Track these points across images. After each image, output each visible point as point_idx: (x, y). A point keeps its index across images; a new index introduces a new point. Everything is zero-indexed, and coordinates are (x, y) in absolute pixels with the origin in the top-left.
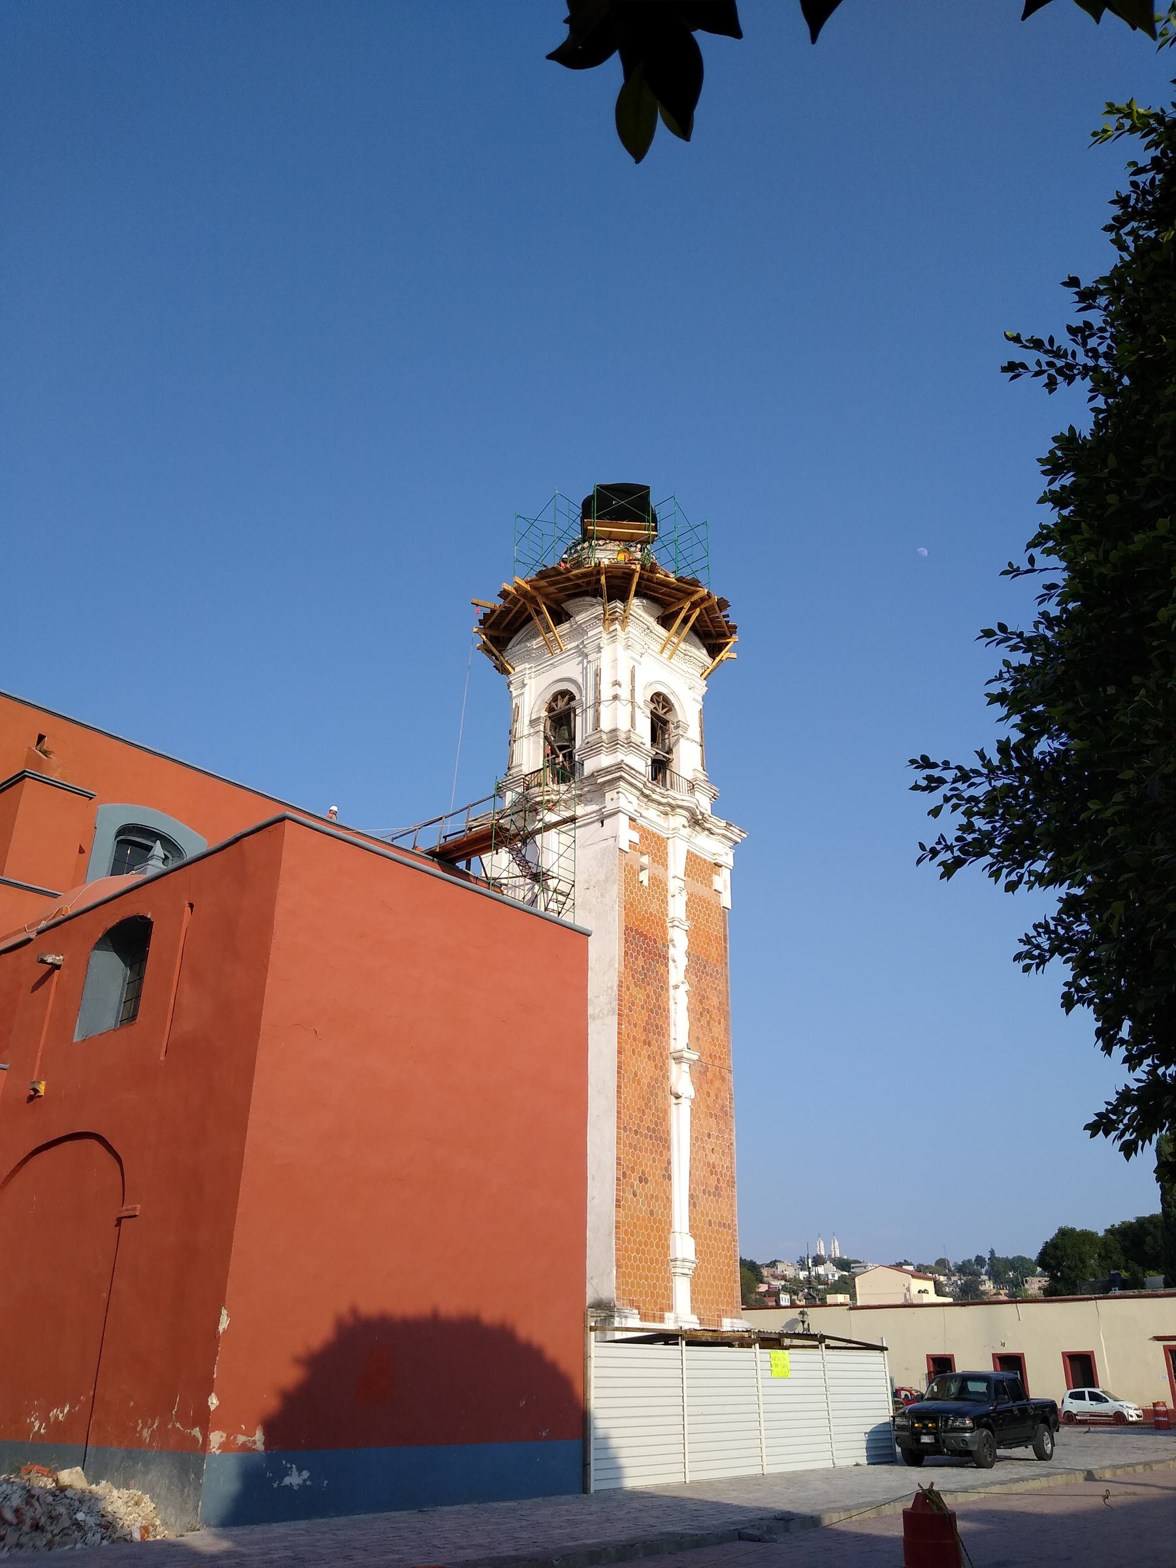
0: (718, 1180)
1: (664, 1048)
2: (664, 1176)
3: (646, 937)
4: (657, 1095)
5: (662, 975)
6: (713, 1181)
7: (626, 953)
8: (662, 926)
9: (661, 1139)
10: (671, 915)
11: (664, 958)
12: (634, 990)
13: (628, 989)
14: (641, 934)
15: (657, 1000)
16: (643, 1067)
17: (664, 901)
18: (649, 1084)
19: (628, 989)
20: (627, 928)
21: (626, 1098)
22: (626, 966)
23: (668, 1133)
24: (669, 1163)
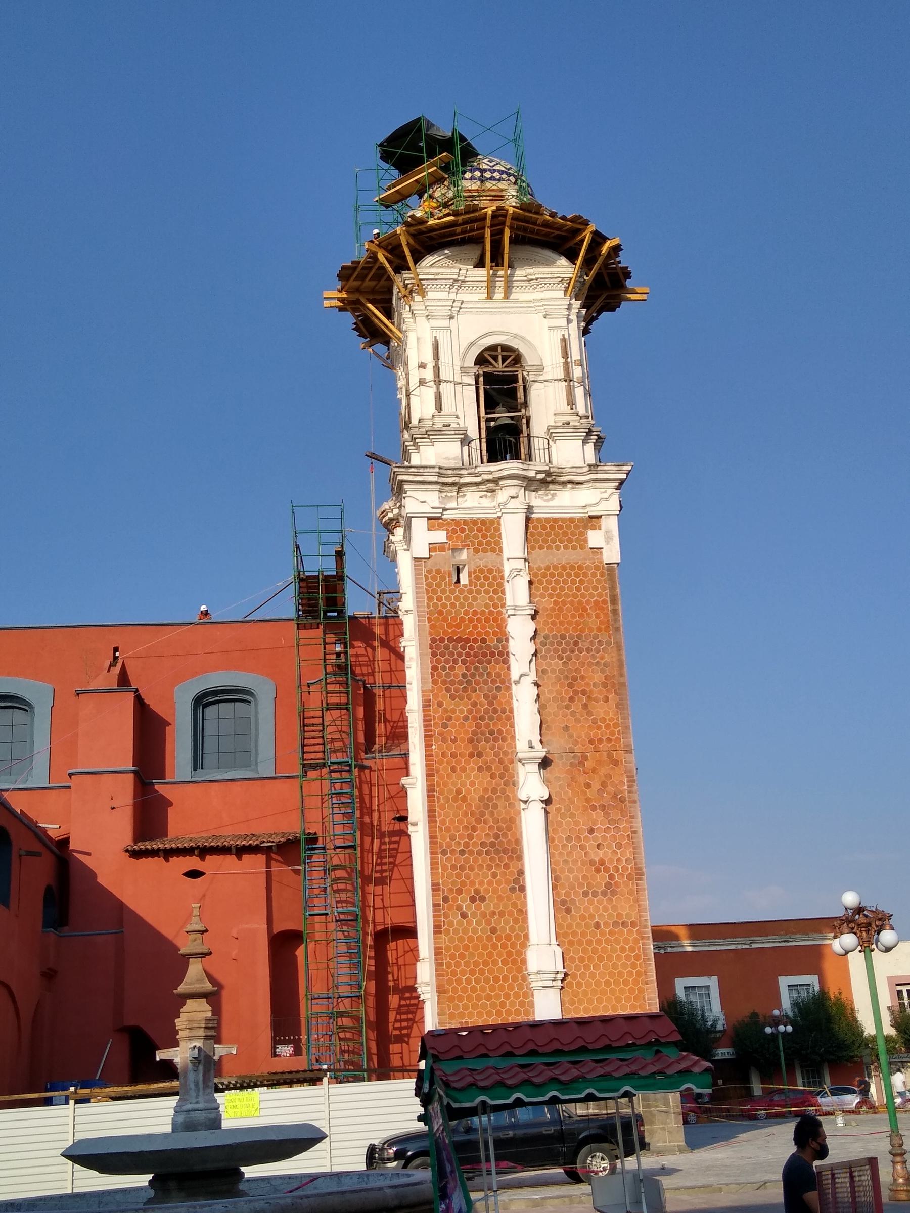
0: (611, 877)
1: (506, 753)
2: (512, 890)
3: (467, 641)
4: (496, 806)
5: (498, 675)
6: (601, 879)
7: (434, 668)
8: (495, 620)
9: (508, 850)
10: (509, 602)
11: (503, 656)
12: (449, 704)
13: (440, 704)
14: (459, 640)
15: (491, 704)
16: (473, 782)
17: (499, 590)
18: (481, 798)
19: (440, 704)
20: (433, 640)
21: (443, 822)
22: (435, 682)
23: (518, 842)
24: (521, 873)
